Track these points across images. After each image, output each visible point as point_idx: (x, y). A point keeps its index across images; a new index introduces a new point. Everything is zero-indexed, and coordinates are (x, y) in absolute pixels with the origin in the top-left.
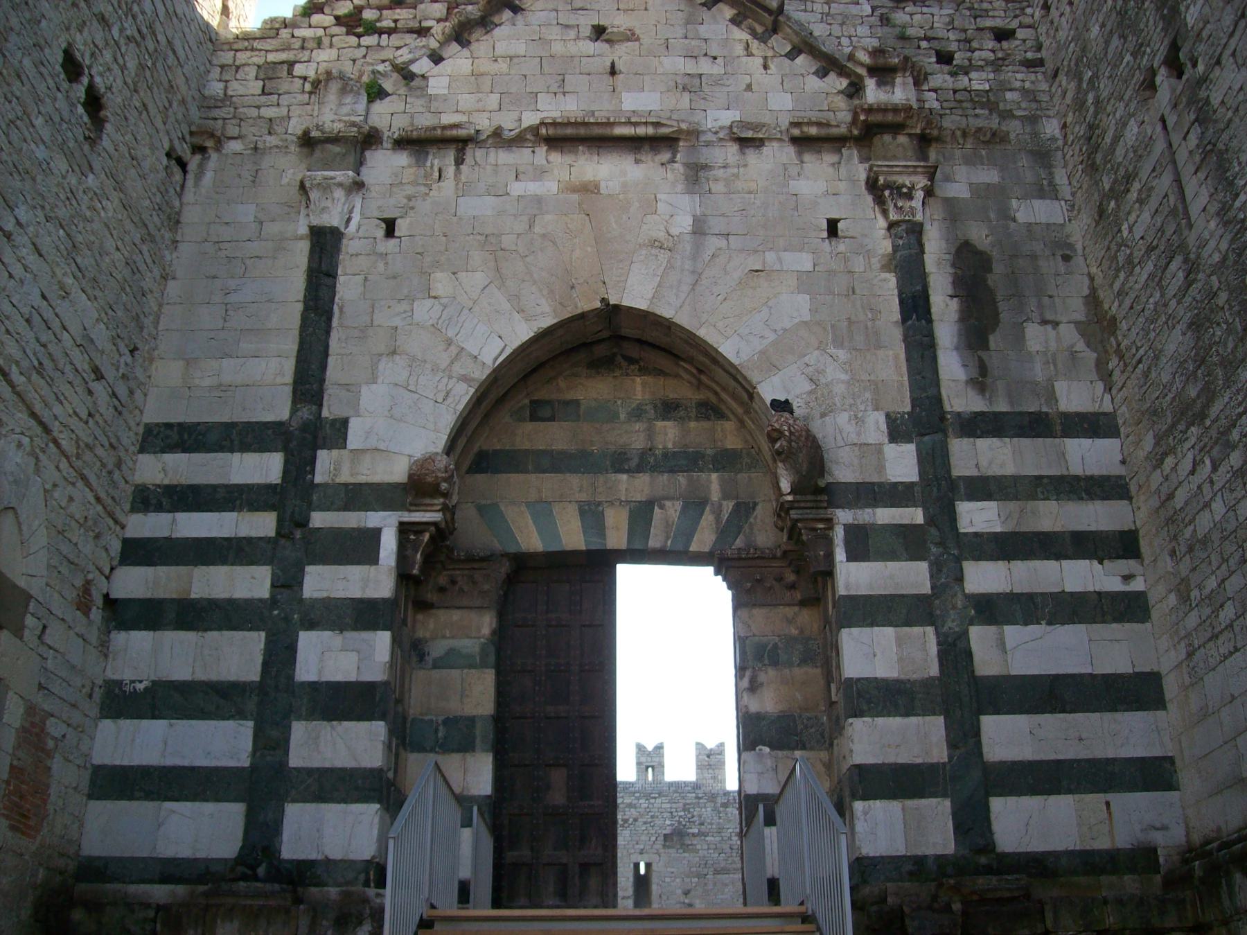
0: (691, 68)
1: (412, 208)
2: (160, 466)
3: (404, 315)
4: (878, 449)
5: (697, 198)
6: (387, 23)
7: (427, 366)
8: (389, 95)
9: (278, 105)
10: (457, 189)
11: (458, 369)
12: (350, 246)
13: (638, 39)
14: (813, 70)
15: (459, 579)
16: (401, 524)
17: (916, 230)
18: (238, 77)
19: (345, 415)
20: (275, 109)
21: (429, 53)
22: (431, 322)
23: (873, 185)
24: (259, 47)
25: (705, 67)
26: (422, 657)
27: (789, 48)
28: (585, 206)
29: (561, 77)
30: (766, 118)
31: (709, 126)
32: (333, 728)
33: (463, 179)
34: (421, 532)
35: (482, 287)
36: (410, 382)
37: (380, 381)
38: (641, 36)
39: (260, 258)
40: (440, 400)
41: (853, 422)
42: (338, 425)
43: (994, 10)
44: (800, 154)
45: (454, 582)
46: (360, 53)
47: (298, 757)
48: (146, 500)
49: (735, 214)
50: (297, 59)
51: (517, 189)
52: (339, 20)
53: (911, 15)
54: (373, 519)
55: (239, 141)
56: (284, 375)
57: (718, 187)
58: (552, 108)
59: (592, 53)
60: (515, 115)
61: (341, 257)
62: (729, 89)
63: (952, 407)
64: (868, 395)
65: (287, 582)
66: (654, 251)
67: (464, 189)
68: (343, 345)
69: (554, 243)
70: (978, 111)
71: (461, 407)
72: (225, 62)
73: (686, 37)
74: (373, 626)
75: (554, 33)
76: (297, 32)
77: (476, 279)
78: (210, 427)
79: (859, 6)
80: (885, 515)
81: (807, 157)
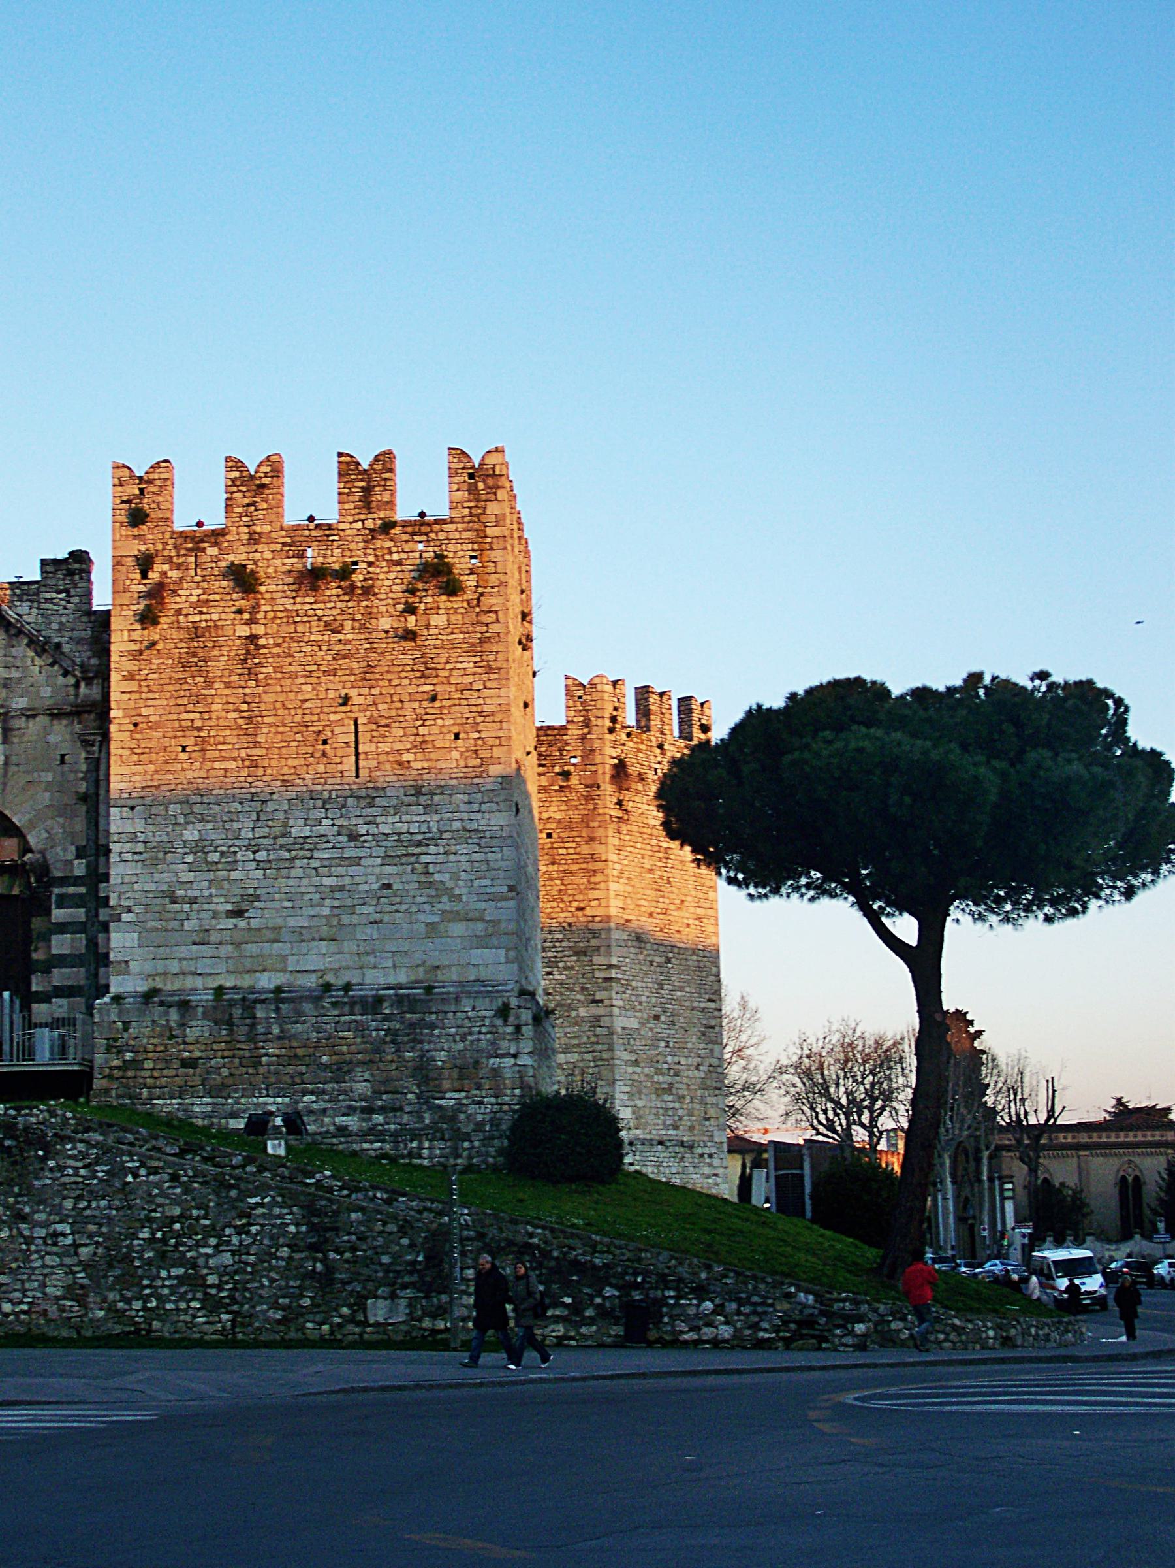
4: (71, 862)
57: (16, 740)
80: (71, 890)
81: (55, 722)
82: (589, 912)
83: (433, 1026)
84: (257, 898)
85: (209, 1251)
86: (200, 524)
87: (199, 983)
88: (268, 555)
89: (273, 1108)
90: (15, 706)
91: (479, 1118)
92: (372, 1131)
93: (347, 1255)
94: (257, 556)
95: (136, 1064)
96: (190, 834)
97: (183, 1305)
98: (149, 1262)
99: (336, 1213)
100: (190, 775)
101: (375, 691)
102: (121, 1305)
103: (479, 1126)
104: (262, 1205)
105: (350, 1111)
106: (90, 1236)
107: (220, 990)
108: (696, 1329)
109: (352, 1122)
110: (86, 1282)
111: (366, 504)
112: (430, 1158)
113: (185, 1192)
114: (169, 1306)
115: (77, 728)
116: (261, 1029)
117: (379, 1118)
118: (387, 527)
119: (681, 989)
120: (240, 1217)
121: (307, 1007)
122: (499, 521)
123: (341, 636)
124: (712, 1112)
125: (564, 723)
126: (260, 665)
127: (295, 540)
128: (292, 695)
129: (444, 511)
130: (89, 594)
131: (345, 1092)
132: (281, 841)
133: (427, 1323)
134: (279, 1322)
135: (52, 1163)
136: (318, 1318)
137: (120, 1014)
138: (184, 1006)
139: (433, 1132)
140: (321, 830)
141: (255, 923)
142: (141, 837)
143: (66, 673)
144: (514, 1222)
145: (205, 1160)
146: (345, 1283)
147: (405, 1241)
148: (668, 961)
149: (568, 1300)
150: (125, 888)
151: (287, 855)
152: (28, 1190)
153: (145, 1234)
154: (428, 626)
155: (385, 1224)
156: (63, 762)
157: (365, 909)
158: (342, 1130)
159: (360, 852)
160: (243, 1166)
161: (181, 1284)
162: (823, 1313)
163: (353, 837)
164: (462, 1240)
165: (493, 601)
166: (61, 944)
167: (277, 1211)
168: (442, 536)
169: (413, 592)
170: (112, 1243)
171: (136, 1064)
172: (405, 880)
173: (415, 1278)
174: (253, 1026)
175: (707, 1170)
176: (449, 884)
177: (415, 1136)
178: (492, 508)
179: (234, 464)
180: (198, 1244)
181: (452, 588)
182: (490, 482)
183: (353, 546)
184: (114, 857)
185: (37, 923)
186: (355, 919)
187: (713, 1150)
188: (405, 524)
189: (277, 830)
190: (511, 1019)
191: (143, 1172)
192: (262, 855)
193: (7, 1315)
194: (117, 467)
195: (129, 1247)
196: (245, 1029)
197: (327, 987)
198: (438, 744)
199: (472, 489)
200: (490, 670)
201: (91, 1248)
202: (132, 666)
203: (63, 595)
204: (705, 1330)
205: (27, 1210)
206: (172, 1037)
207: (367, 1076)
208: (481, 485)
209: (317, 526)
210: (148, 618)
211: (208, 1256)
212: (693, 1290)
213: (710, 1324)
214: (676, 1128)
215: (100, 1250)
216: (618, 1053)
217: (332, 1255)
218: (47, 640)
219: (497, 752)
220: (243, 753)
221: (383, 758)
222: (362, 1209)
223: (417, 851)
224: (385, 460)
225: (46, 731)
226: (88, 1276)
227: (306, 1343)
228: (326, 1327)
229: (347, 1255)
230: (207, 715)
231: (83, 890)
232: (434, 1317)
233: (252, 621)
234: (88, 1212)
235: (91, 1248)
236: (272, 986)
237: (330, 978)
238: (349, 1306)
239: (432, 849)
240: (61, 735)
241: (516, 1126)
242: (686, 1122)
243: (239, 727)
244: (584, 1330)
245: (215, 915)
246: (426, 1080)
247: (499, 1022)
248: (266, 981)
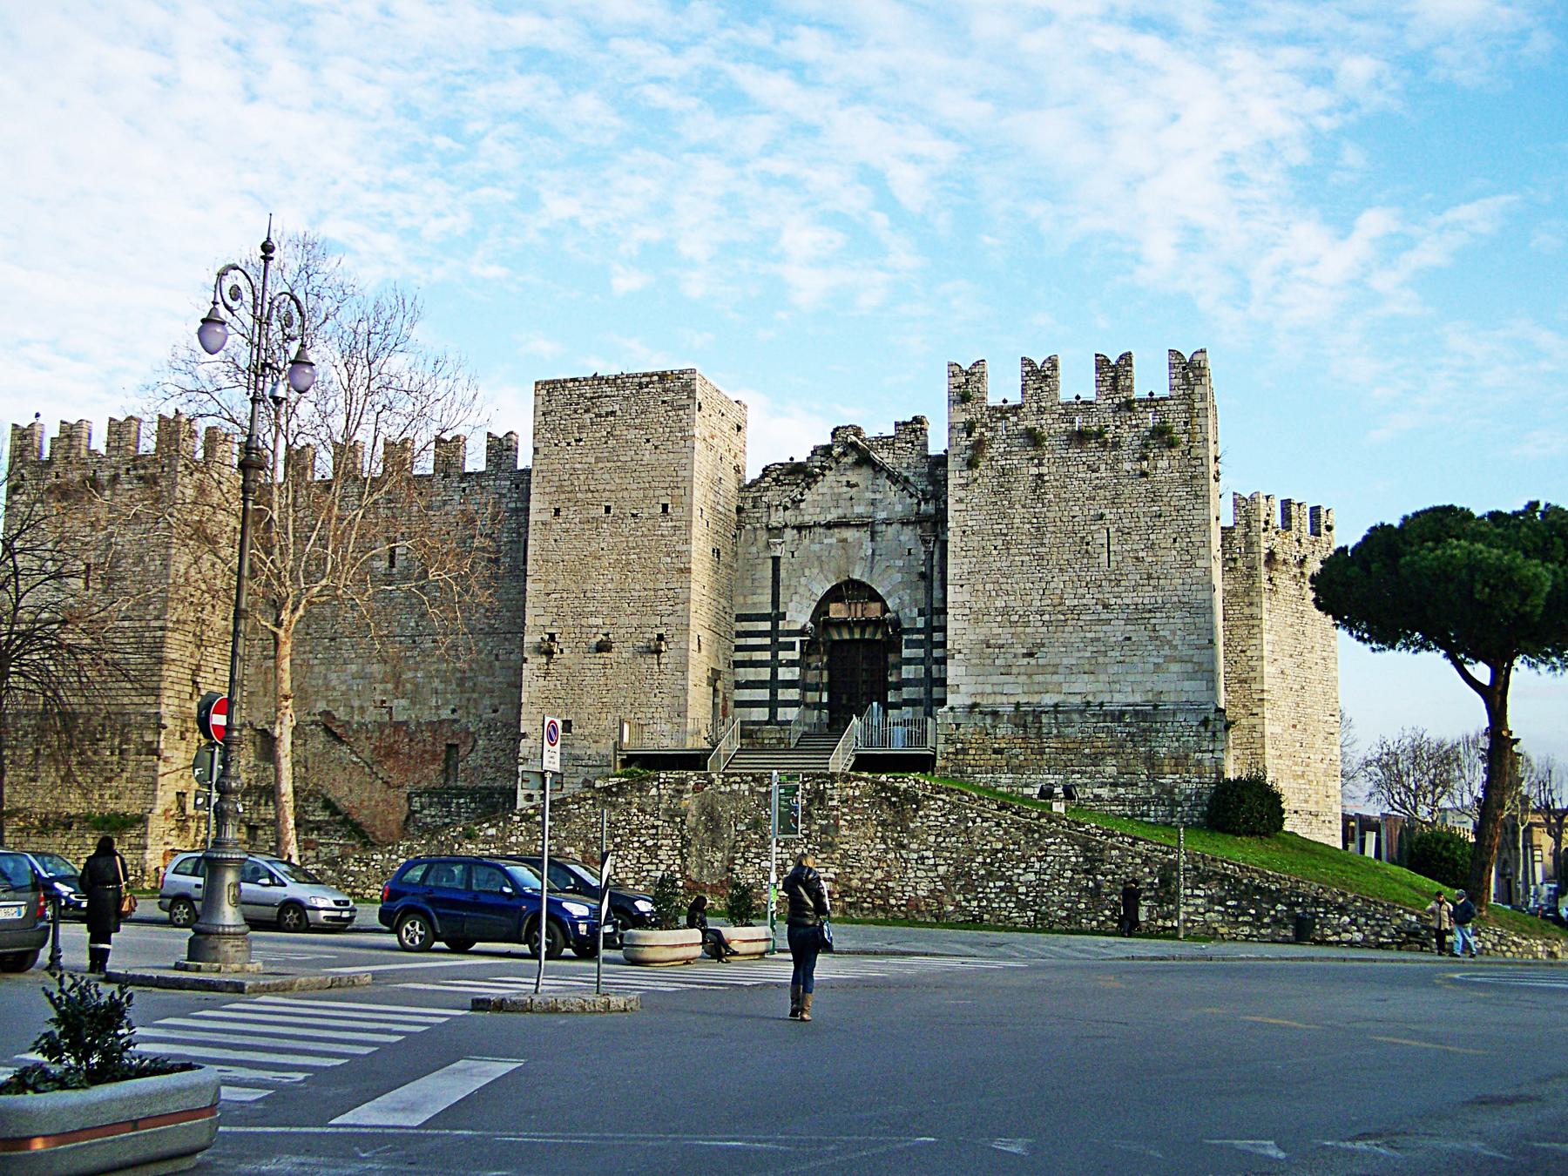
0: (873, 496)
12: (782, 560)
17: (932, 553)
25: (878, 496)
30: (893, 516)
47: (780, 698)
48: (739, 635)
51: (826, 541)
52: (774, 480)
54: (793, 639)
58: (832, 516)
65: (775, 656)
67: (812, 541)
75: (835, 484)
77: (816, 571)
80: (915, 637)
82: (1249, 653)
83: (1158, 731)
84: (1043, 645)
85: (1021, 871)
86: (1005, 401)
87: (1004, 699)
88: (1050, 421)
89: (1053, 782)
91: (1188, 792)
92: (1117, 798)
93: (1110, 877)
94: (1043, 422)
95: (964, 751)
96: (1000, 603)
97: (1003, 905)
98: (982, 877)
99: (1102, 851)
100: (999, 564)
101: (1120, 511)
102: (964, 903)
103: (1188, 798)
104: (1052, 843)
105: (1102, 785)
106: (945, 859)
107: (1018, 705)
108: (1338, 934)
109: (1104, 792)
110: (942, 888)
111: (1115, 387)
112: (1156, 817)
113: (1006, 833)
114: (995, 905)
115: (919, 531)
116: (1045, 730)
117: (1121, 790)
118: (1128, 405)
119: (1311, 707)
120: (1041, 850)
121: (1075, 717)
122: (1203, 398)
123: (1098, 475)
124: (1331, 792)
125: (1231, 524)
126: (1045, 493)
127: (1068, 411)
128: (1066, 513)
129: (1166, 393)
130: (925, 445)
131: (1100, 773)
132: (1060, 608)
133: (1160, 922)
134: (1063, 918)
135: (921, 813)
136: (1090, 916)
137: (954, 718)
138: (995, 714)
139: (1158, 800)
140: (1085, 601)
141: (1041, 661)
142: (968, 605)
143: (911, 496)
144: (1214, 860)
145: (1014, 813)
146: (1108, 895)
147: (1147, 870)
148: (1303, 688)
149: (1253, 912)
150: (956, 638)
151: (1062, 617)
152: (905, 829)
153: (980, 859)
154: (1156, 468)
155: (1133, 858)
156: (909, 553)
157: (1113, 653)
158: (1097, 797)
159: (1111, 616)
160: (1038, 818)
161: (1002, 891)
162: (1424, 928)
163: (1105, 606)
164: (1185, 870)
165: (1199, 451)
166: (908, 672)
167: (1064, 847)
168: (1165, 408)
169: (1146, 446)
170: (958, 864)
171: (964, 751)
172: (1140, 634)
173: (1152, 893)
174: (1040, 728)
175: (1328, 832)
176: (1169, 638)
177: (1146, 802)
178: (1198, 389)
179: (1027, 362)
180: (1013, 867)
181: (1172, 444)
182: (1197, 372)
183: (1106, 415)
184: (949, 618)
185: (892, 658)
186: (1107, 660)
187: (1332, 818)
188: (1141, 400)
189: (1056, 601)
190: (1210, 727)
191: (979, 820)
192: (1046, 617)
193: (893, 906)
194: (950, 365)
195: (970, 867)
196: (1035, 731)
197: (1088, 704)
198: (1162, 545)
199: (1185, 377)
200: (1197, 497)
201: (945, 868)
202: (962, 494)
204: (1343, 935)
205: (906, 841)
206: (987, 734)
207: (1114, 762)
208: (1191, 375)
209: (1083, 403)
210: (971, 464)
211: (1019, 875)
212: (1335, 909)
213: (1346, 931)
214: (1306, 802)
215: (951, 869)
216: (1267, 750)
217: (1099, 877)
218: (900, 474)
219: (1202, 551)
220: (1034, 551)
221: (1126, 554)
222: (1119, 848)
223: (1148, 615)
224: (1126, 358)
225: (899, 533)
226: (943, 884)
227: (1081, 932)
228: (1094, 923)
229: (1110, 877)
230: (1010, 526)
231: (923, 637)
232: (1165, 919)
233: (1040, 464)
234: (943, 845)
235: (945, 868)
236: (1051, 703)
237: (1090, 698)
238: (1110, 910)
239: (1158, 615)
240: (908, 536)
241: (1212, 799)
242: (1314, 798)
243: (1031, 534)
244: (1263, 931)
245: (1015, 656)
246: (1153, 766)
247: (1202, 729)
248: (1049, 699)
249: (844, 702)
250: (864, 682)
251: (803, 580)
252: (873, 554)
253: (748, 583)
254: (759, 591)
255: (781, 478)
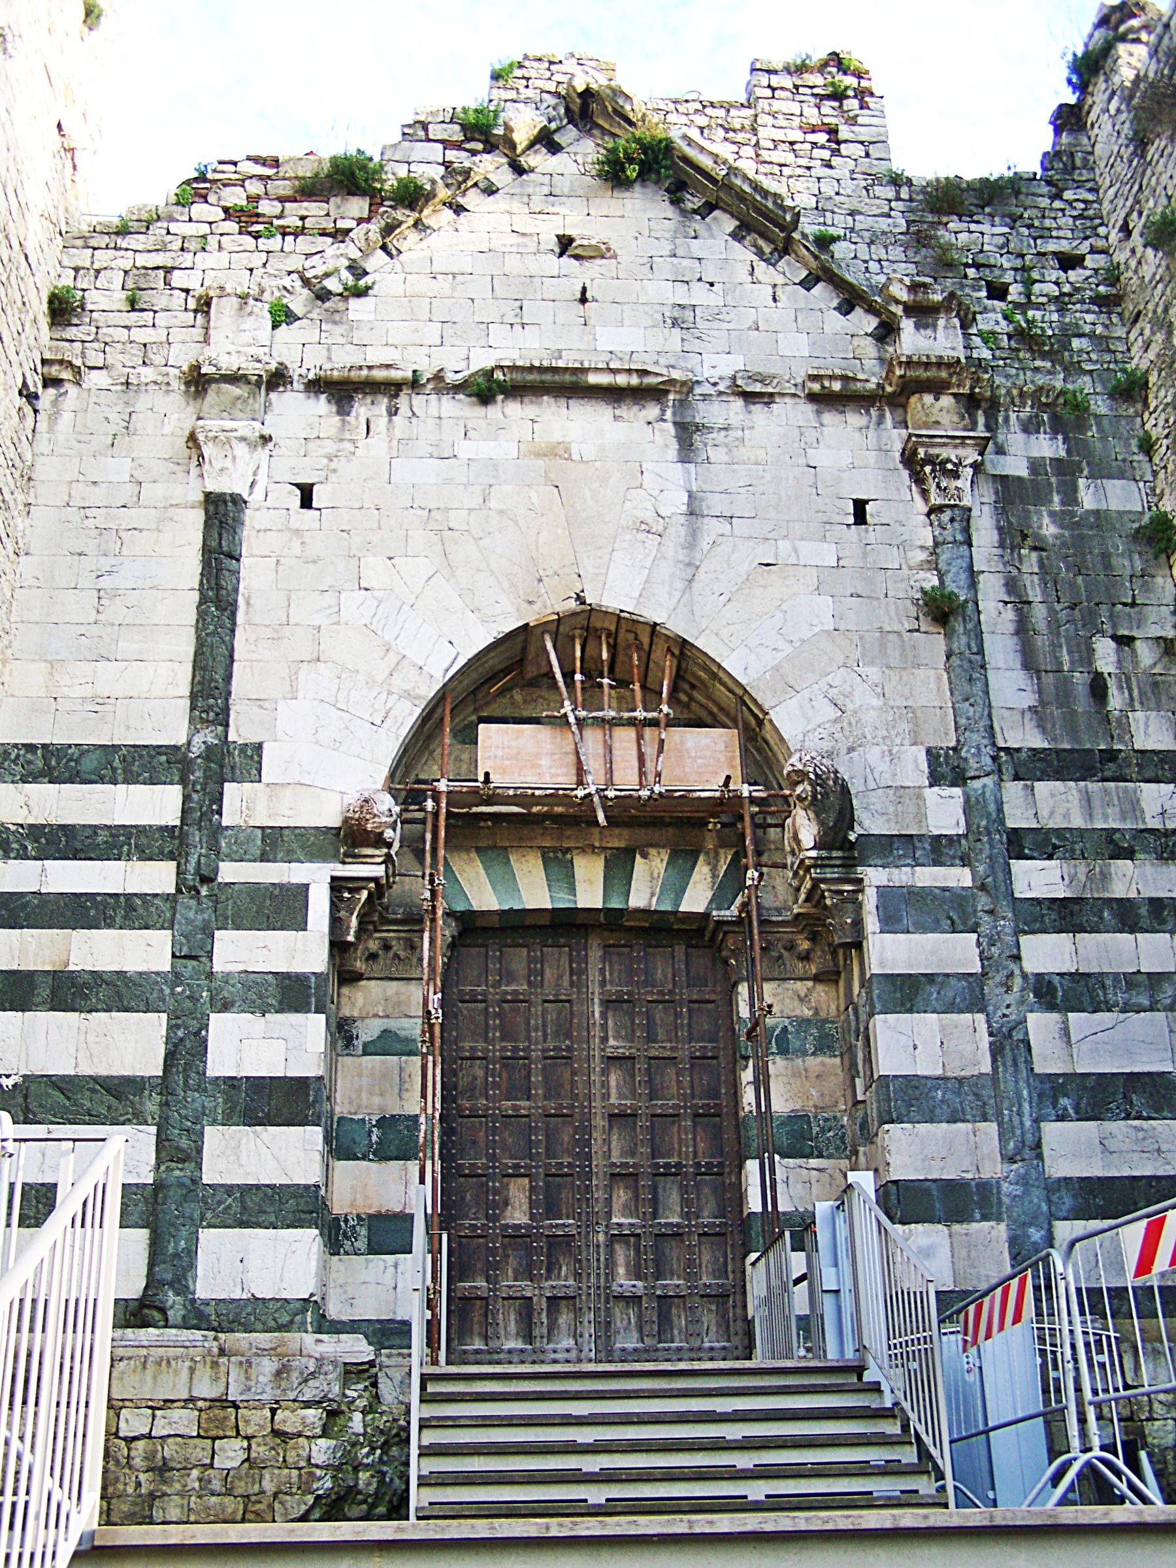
0: (681, 295)
1: (334, 471)
2: (22, 800)
3: (329, 611)
5: (691, 466)
6: (293, 222)
7: (359, 677)
8: (299, 319)
9: (154, 325)
10: (390, 448)
11: (398, 683)
12: (252, 519)
13: (615, 257)
14: (835, 303)
15: (394, 943)
16: (333, 878)
17: (965, 516)
18: (98, 285)
19: (257, 740)
20: (150, 330)
21: (347, 263)
22: (364, 621)
23: (909, 459)
24: (124, 245)
25: (699, 295)
26: (349, 1040)
27: (804, 273)
28: (552, 476)
29: (518, 304)
31: (706, 376)
32: (254, 1132)
33: (398, 434)
34: (358, 890)
35: (426, 578)
36: (339, 698)
37: (300, 695)
38: (618, 252)
39: (141, 531)
40: (378, 722)
41: (887, 759)
42: (249, 753)
43: (1059, 228)
44: (819, 413)
45: (387, 947)
46: (258, 259)
47: (216, 1169)
49: (740, 490)
50: (176, 265)
51: (465, 449)
53: (956, 233)
55: (104, 372)
56: (177, 685)
59: (556, 274)
60: (463, 353)
61: (245, 533)
62: (730, 326)
63: (1006, 741)
64: (904, 726)
66: (642, 536)
68: (253, 648)
69: (516, 523)
70: (1038, 363)
71: (404, 731)
72: (81, 264)
73: (675, 255)
74: (300, 1006)
76: (173, 227)
78: (84, 750)
79: (890, 221)
80: (927, 876)
90: (707, 373)
156: (860, 516)
203: (821, 138)
231: (960, 877)
249: (518, 1215)
250: (617, 1117)
251: (353, 604)
252: (693, 512)
253: (79, 607)
254: (128, 645)
255: (267, 208)
